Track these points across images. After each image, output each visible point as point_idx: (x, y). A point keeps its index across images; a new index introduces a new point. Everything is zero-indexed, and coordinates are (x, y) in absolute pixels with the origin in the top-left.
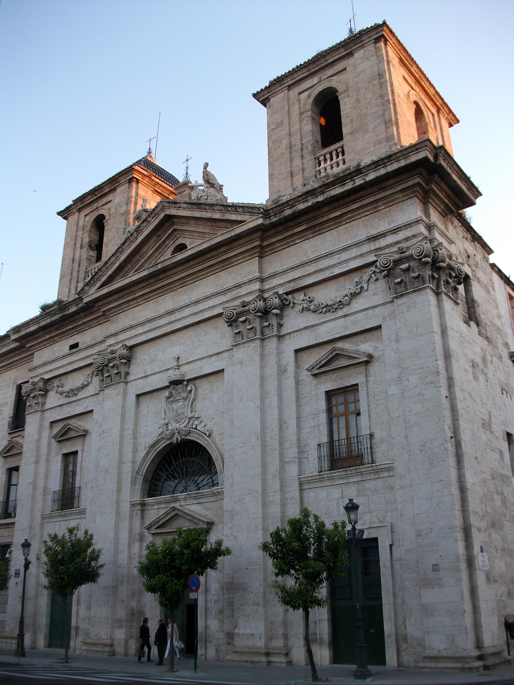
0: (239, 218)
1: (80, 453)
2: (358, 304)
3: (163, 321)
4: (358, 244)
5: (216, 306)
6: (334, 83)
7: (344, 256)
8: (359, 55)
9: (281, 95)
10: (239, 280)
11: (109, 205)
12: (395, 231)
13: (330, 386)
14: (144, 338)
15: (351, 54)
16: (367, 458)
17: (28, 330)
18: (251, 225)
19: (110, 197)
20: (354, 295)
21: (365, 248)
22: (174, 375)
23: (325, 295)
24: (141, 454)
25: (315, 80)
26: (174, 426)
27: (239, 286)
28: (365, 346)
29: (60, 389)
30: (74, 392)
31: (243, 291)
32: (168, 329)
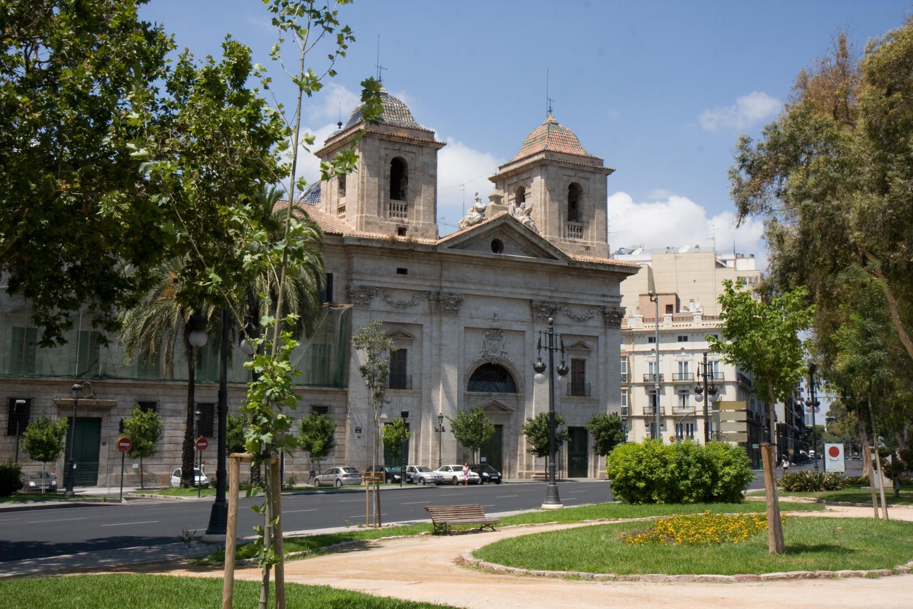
0: (555, 256)
1: (409, 351)
2: (591, 323)
3: (489, 288)
4: (597, 295)
5: (527, 294)
6: (582, 182)
7: (590, 298)
8: (598, 176)
9: (555, 169)
10: (542, 288)
11: (413, 155)
12: (612, 297)
13: (574, 357)
14: (473, 292)
15: (594, 173)
16: (587, 393)
17: (370, 245)
18: (562, 264)
19: (414, 149)
20: (590, 318)
21: (599, 298)
22: (496, 325)
23: (577, 312)
24: (468, 365)
25: (573, 173)
26: (491, 354)
27: (540, 289)
28: (589, 343)
29: (389, 299)
30: (404, 306)
31: (542, 293)
32: (492, 294)
